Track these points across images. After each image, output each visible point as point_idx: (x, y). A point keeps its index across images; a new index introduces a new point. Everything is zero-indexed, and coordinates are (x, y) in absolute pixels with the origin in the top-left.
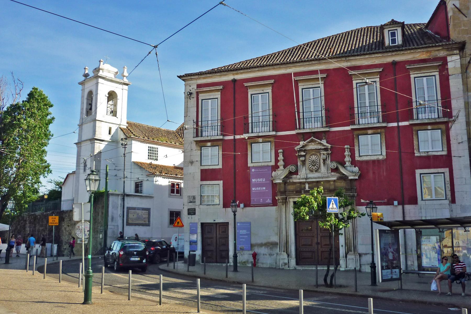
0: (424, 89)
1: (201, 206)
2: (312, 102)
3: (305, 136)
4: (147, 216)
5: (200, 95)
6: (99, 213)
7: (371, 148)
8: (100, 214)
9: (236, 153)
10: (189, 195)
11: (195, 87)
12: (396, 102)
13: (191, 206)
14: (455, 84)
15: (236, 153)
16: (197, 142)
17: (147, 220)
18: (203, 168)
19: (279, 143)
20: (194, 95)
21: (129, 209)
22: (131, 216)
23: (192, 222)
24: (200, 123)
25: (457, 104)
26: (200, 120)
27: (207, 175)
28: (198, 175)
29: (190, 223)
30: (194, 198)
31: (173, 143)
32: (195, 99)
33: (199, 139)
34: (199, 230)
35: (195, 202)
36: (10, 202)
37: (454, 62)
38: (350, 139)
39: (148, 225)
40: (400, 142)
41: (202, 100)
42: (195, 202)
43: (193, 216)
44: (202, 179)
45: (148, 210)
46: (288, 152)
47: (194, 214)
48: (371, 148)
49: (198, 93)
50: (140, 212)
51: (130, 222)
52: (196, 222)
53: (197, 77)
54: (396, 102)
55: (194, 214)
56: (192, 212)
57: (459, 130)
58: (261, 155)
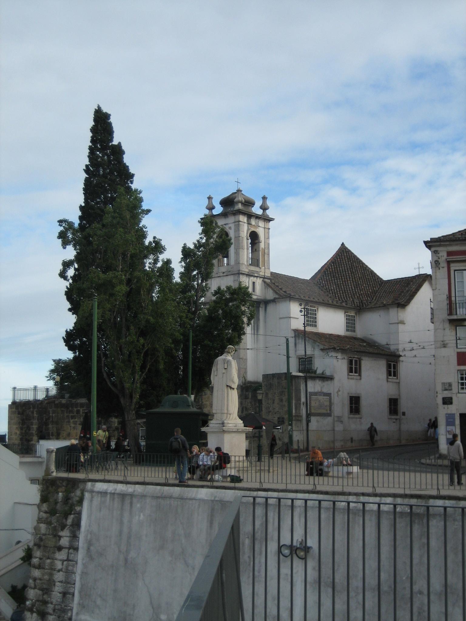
1: (459, 395)
4: (327, 403)
5: (452, 265)
6: (274, 400)
8: (277, 400)
10: (443, 381)
11: (445, 254)
13: (447, 394)
16: (451, 321)
17: (328, 408)
18: (459, 350)
20: (444, 264)
21: (312, 394)
22: (313, 404)
23: (449, 412)
24: (453, 299)
26: (453, 294)
28: (454, 359)
29: (446, 414)
30: (450, 385)
31: (330, 301)
32: (446, 269)
33: (455, 317)
34: (458, 422)
35: (451, 390)
36: (258, 392)
39: (329, 415)
41: (455, 270)
42: (451, 390)
43: (450, 406)
44: (459, 364)
45: (329, 395)
47: (451, 403)
49: (449, 263)
50: (321, 398)
51: (313, 411)
52: (453, 412)
53: (448, 243)
55: (451, 403)
56: (447, 401)
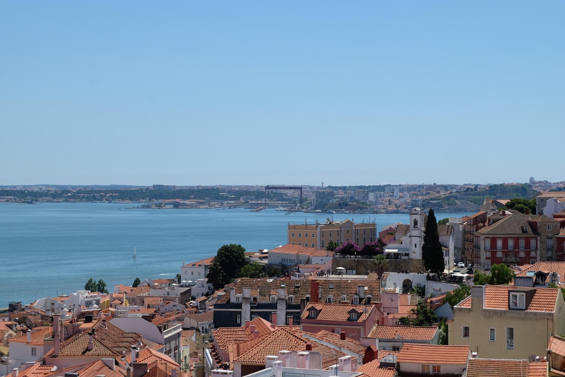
0: (533, 243)
2: (511, 243)
3: (510, 251)
7: (522, 254)
9: (494, 254)
12: (528, 245)
14: (539, 243)
15: (494, 254)
19: (503, 252)
25: (539, 247)
27: (487, 258)
37: (539, 238)
38: (518, 252)
40: (528, 254)
46: (506, 254)
48: (522, 254)
54: (528, 245)
57: (538, 252)
58: (499, 254)
